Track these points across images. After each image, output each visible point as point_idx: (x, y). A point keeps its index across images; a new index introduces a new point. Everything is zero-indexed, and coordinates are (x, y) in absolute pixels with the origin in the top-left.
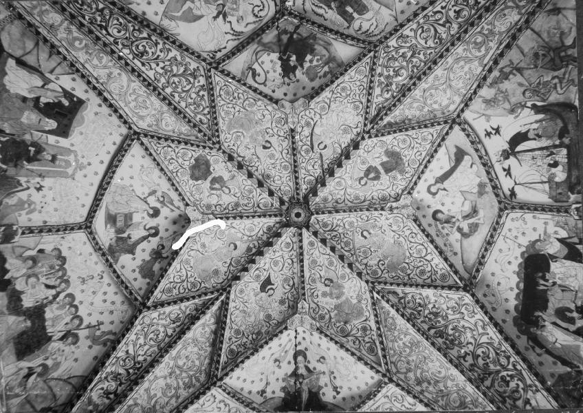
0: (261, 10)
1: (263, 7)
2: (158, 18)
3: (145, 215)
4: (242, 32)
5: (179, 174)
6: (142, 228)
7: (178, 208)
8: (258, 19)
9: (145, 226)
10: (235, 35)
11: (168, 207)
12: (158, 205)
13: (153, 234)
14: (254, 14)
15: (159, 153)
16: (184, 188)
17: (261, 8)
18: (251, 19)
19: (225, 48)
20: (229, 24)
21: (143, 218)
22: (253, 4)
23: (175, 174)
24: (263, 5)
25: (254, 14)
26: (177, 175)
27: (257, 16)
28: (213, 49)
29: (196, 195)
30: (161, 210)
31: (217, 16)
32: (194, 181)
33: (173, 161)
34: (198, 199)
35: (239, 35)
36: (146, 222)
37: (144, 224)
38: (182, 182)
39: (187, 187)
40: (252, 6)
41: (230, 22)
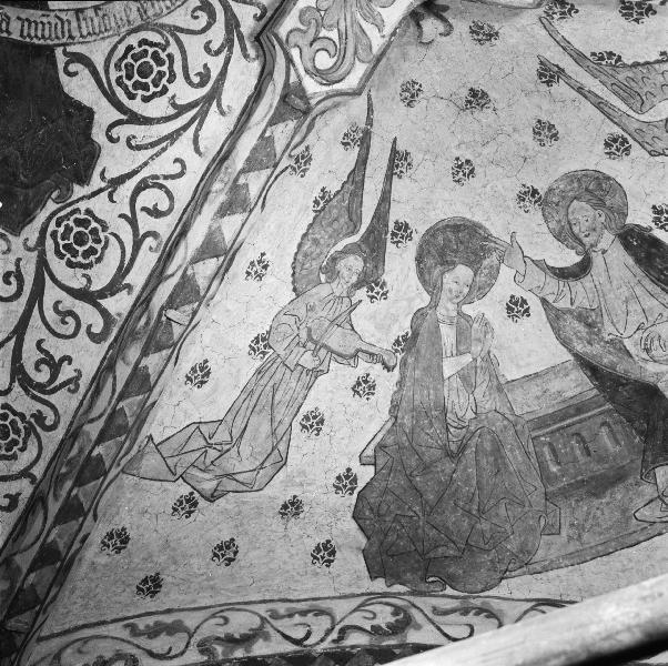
3: (490, 308)
5: (102, 276)
6: (580, 294)
7: (361, 139)
9: (562, 274)
11: (385, 198)
12: (400, 263)
13: (599, 203)
15: (24, 488)
16: (183, 189)
21: (516, 308)
23: (119, 304)
26: (112, 289)
29: (198, 59)
30: (420, 228)
32: (98, 135)
33: (30, 355)
34: (217, 34)
36: (537, 277)
37: (553, 285)
38: (146, 223)
39: (164, 165)
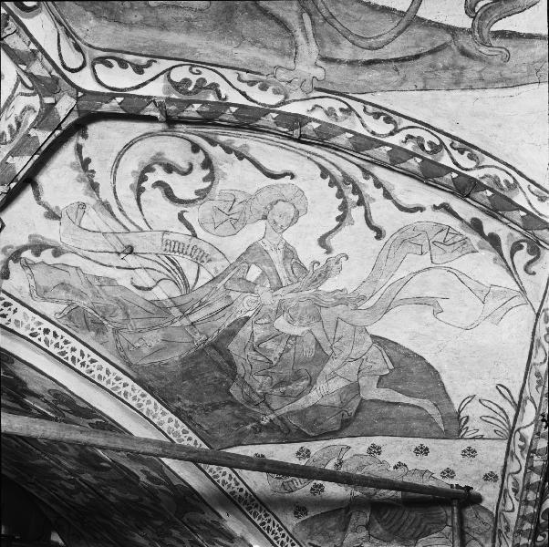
0: (169, 168)
1: (149, 169)
2: (479, 445)
4: (325, 173)
8: (216, 152)
10: (356, 190)
14: (211, 178)
17: (159, 174)
18: (236, 176)
19: (445, 208)
20: (333, 241)
22: (181, 217)
24: (142, 178)
25: (211, 178)
27: (208, 164)
28: (487, 255)
31: (341, 299)
35: (348, 179)
40: (192, 215)
41: (323, 242)
